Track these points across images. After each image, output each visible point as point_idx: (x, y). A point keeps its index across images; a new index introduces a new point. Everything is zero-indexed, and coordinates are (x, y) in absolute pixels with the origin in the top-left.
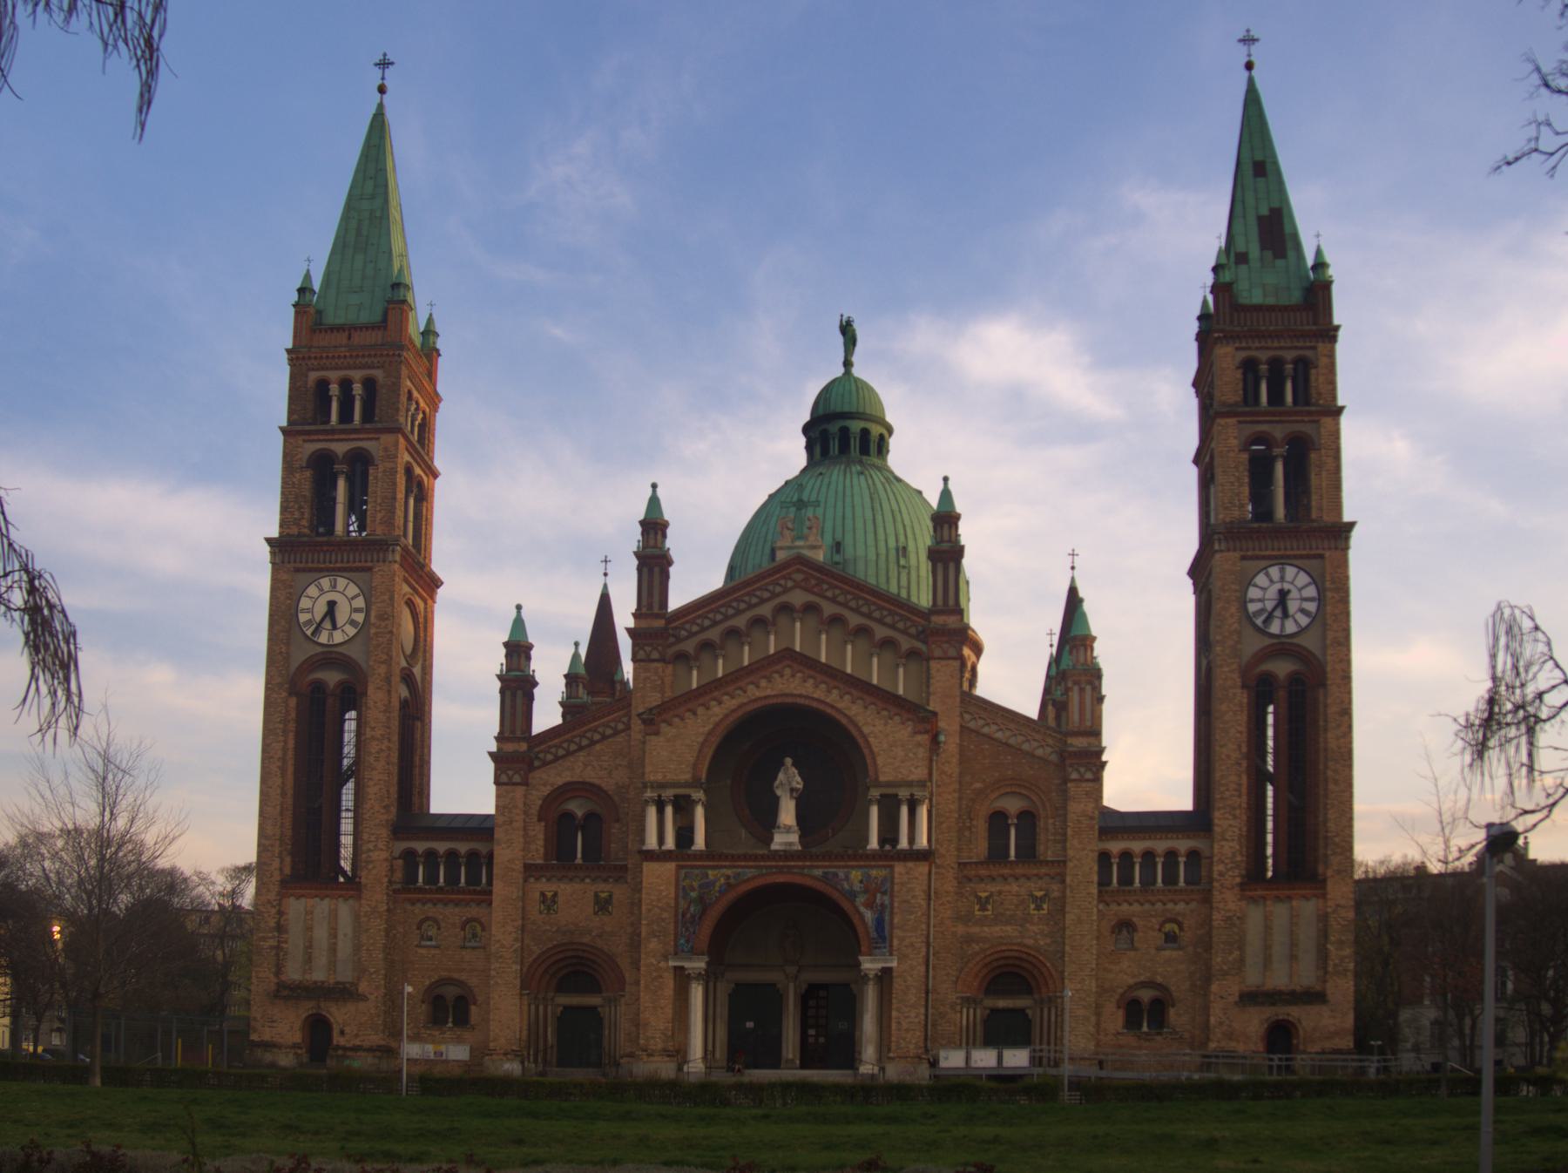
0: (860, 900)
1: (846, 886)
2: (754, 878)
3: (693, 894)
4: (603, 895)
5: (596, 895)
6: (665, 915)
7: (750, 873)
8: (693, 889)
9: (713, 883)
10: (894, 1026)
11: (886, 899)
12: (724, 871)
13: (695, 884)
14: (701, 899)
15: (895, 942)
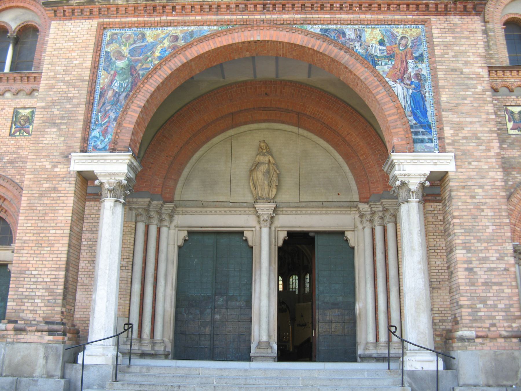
0: (384, 68)
1: (359, 49)
2: (213, 36)
3: (121, 64)
4: (25, 112)
5: (16, 112)
6: (74, 93)
7: (206, 30)
8: (120, 55)
9: (154, 46)
10: (461, 276)
11: (424, 68)
12: (171, 30)
13: (125, 50)
14: (131, 69)
15: (448, 132)
